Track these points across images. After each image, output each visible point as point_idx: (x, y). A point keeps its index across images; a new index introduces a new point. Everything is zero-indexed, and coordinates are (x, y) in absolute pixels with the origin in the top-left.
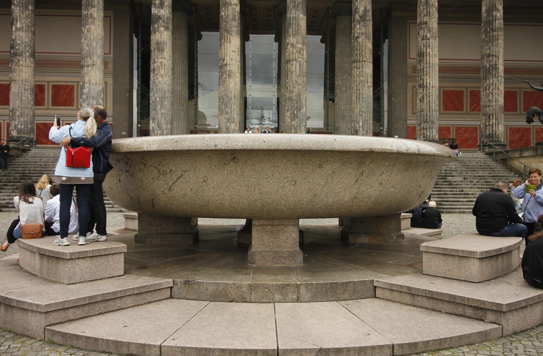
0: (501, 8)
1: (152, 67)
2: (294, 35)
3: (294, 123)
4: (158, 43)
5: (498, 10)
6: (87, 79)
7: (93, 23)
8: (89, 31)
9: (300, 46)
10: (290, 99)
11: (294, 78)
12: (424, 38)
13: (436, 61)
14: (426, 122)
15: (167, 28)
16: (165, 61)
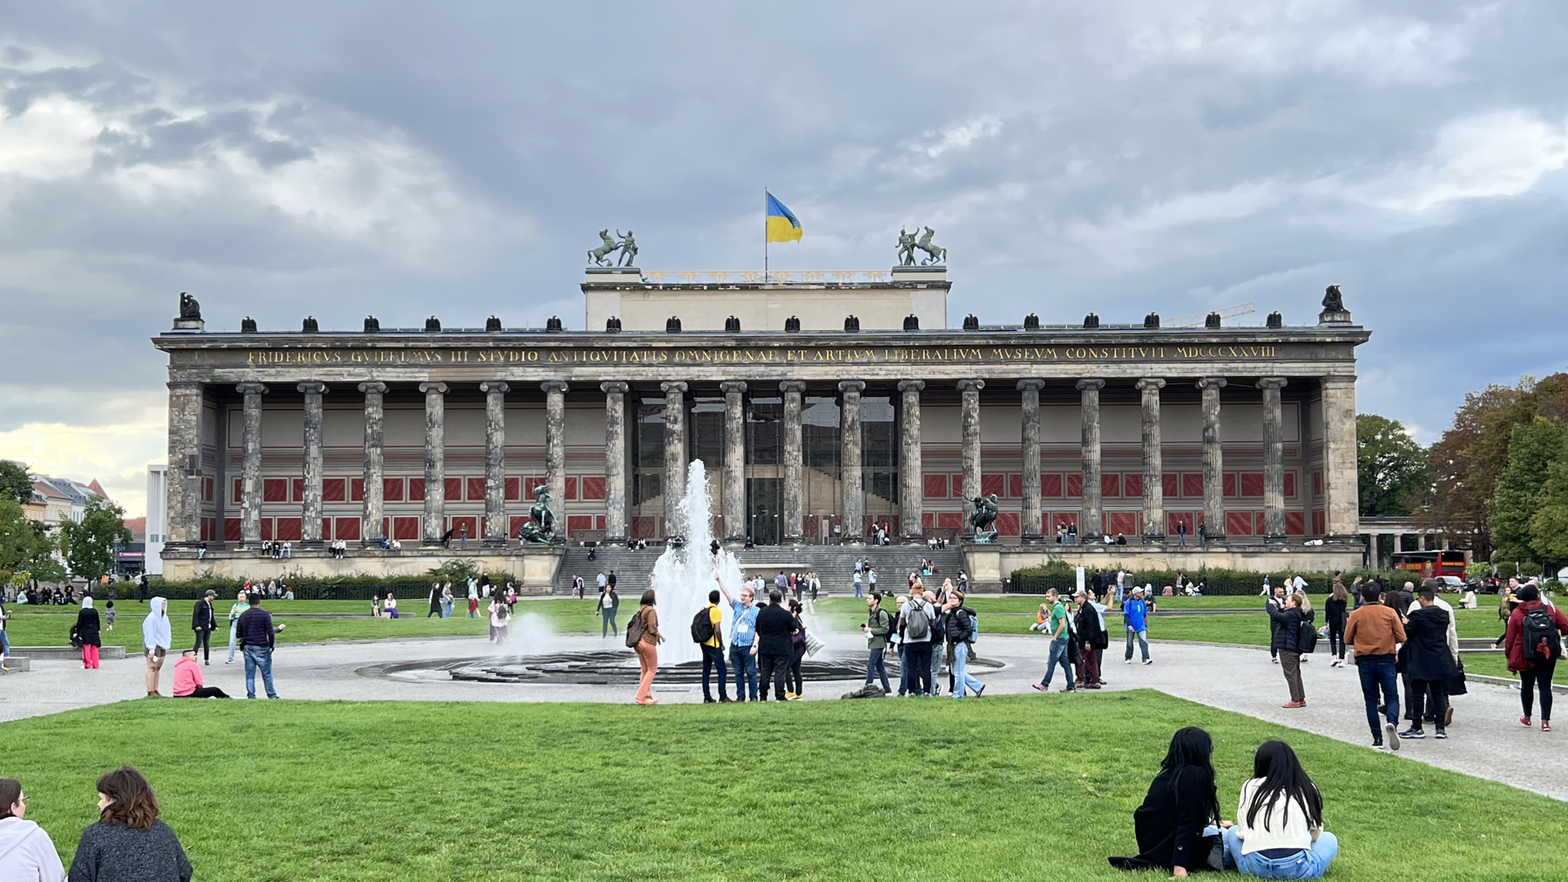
0: (975, 415)
1: (667, 474)
2: (791, 444)
3: (791, 521)
4: (673, 454)
5: (973, 417)
6: (613, 487)
7: (617, 438)
8: (614, 445)
9: (795, 453)
10: (788, 500)
11: (791, 482)
12: (907, 444)
13: (919, 463)
14: (909, 518)
15: (680, 440)
16: (678, 469)
